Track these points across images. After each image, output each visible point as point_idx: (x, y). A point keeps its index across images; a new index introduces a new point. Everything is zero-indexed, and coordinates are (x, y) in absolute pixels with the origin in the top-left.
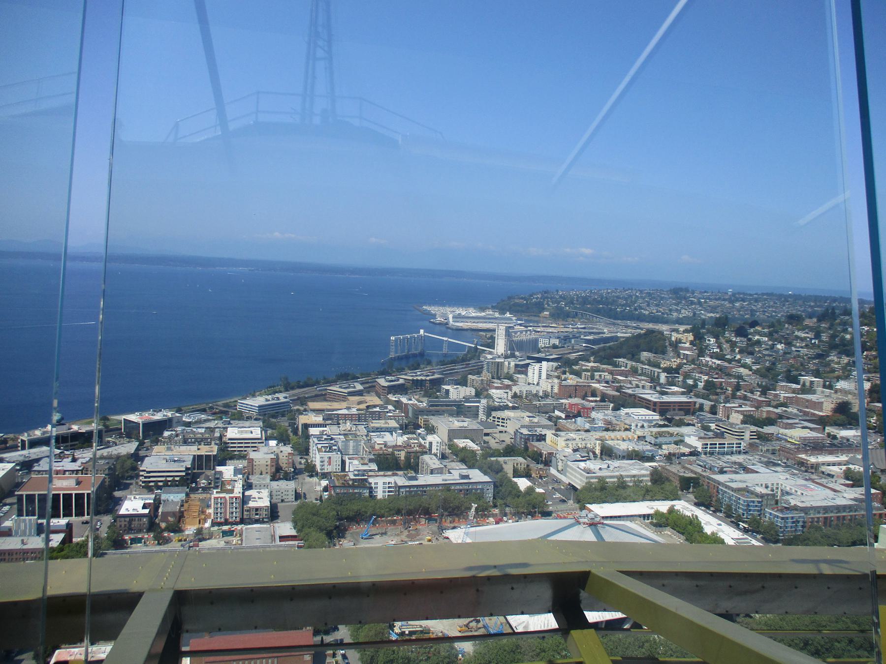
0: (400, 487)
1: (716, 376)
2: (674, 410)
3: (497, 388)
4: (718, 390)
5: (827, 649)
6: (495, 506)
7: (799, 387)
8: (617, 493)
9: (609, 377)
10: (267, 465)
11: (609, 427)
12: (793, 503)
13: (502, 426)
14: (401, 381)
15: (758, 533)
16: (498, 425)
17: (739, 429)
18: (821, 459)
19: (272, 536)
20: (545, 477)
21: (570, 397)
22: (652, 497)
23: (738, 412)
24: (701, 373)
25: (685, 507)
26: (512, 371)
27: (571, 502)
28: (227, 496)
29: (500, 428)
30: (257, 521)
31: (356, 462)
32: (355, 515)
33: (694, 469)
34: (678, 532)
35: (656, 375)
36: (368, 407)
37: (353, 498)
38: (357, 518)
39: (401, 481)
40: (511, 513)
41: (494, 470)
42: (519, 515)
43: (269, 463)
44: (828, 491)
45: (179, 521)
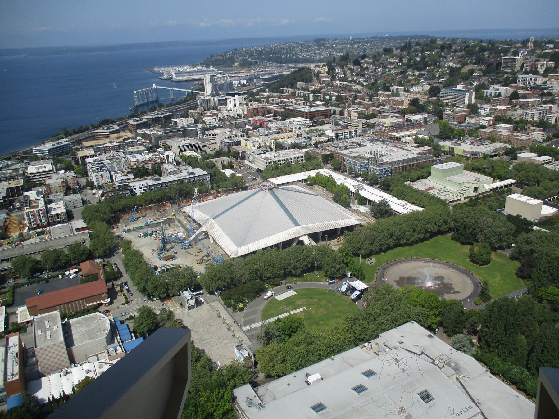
0: (150, 186)
1: (343, 92)
2: (318, 116)
3: (208, 116)
4: (345, 101)
5: (402, 236)
6: (212, 189)
7: (390, 93)
8: (285, 170)
9: (278, 100)
10: (60, 187)
11: (280, 131)
12: (385, 160)
13: (213, 140)
14: (145, 120)
15: (367, 180)
16: (211, 139)
17: (356, 122)
18: (402, 134)
19: (71, 230)
20: (242, 167)
21: (255, 116)
22: (306, 169)
23: (356, 112)
24: (334, 91)
25: (325, 172)
26: (217, 104)
27: (259, 179)
28: (35, 210)
29: (212, 141)
30: (59, 222)
31: (119, 175)
32: (124, 208)
33: (331, 149)
34: (322, 186)
35: (307, 95)
36: (124, 140)
37: (120, 197)
38: (126, 209)
39: (150, 182)
40: (223, 191)
41: (210, 167)
42: (228, 191)
43: (61, 185)
44: (405, 151)
45: (6, 231)
